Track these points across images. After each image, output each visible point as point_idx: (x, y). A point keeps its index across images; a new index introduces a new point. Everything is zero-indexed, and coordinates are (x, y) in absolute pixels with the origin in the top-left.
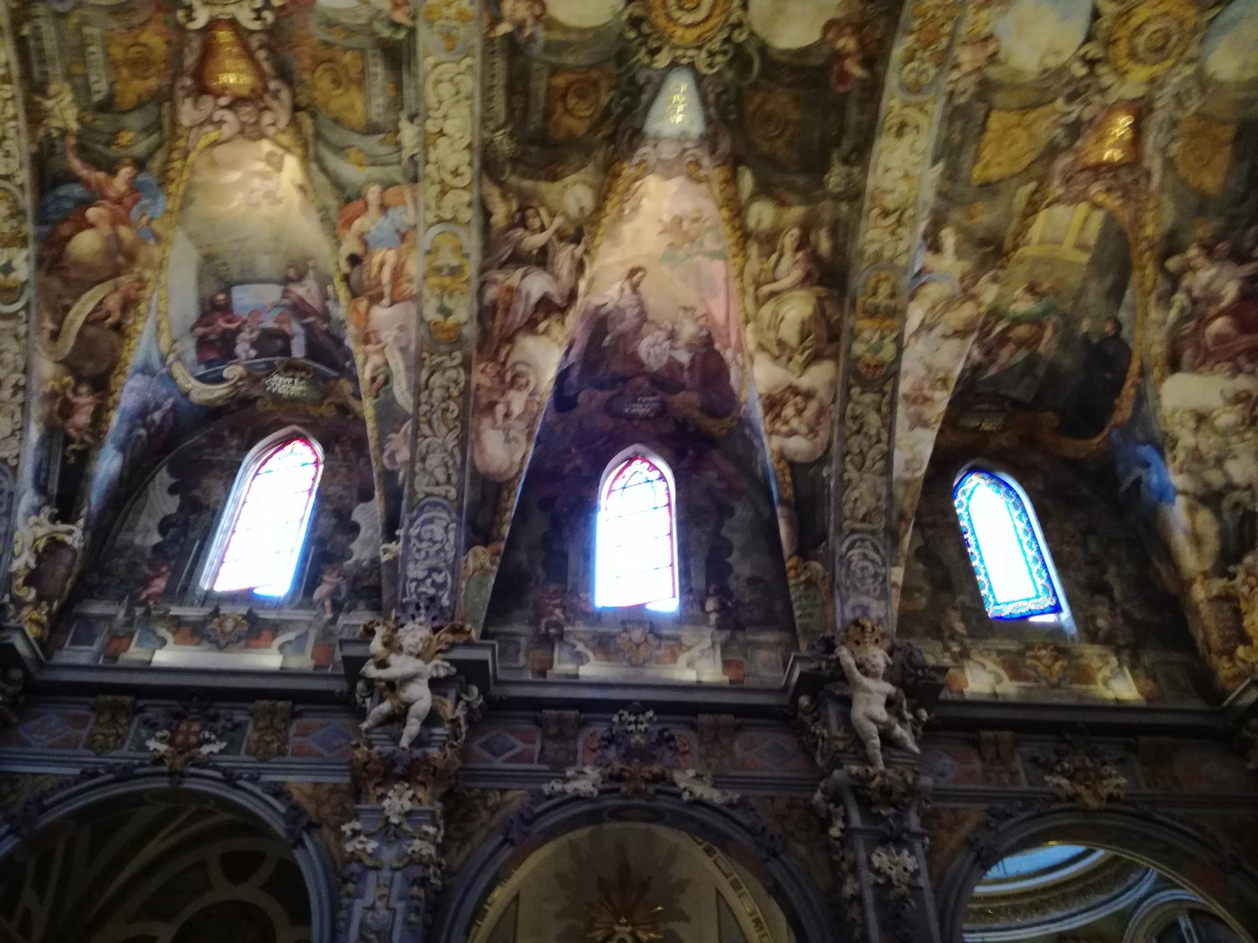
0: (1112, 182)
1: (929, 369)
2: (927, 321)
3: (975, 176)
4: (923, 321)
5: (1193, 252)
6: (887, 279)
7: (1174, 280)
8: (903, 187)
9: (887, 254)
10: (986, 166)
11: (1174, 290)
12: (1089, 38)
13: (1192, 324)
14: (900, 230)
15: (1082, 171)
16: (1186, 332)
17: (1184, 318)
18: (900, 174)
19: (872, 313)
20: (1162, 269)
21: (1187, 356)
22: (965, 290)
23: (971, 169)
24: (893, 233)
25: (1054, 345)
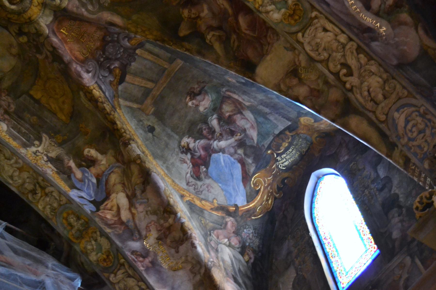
0: (121, 37)
1: (154, 213)
2: (129, 194)
3: (63, 118)
4: (128, 196)
5: (186, 13)
6: (68, 214)
7: (197, 35)
8: (25, 175)
9: (55, 205)
10: (61, 110)
11: (202, 37)
12: (6, 28)
13: (234, 37)
14: (47, 191)
15: (104, 51)
16: (236, 44)
17: (225, 41)
18: (17, 174)
19: (80, 236)
20: (185, 39)
21: (250, 53)
22: (124, 163)
23: (58, 119)
24: (46, 195)
25: (246, 97)
